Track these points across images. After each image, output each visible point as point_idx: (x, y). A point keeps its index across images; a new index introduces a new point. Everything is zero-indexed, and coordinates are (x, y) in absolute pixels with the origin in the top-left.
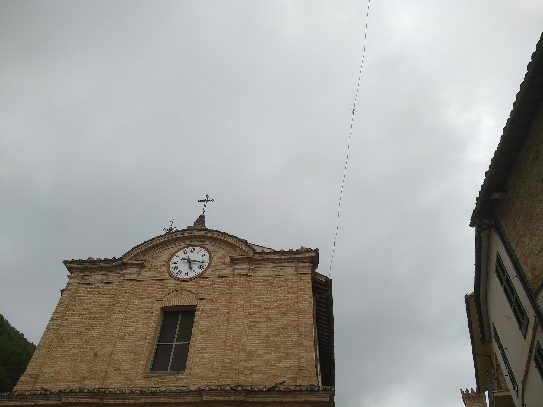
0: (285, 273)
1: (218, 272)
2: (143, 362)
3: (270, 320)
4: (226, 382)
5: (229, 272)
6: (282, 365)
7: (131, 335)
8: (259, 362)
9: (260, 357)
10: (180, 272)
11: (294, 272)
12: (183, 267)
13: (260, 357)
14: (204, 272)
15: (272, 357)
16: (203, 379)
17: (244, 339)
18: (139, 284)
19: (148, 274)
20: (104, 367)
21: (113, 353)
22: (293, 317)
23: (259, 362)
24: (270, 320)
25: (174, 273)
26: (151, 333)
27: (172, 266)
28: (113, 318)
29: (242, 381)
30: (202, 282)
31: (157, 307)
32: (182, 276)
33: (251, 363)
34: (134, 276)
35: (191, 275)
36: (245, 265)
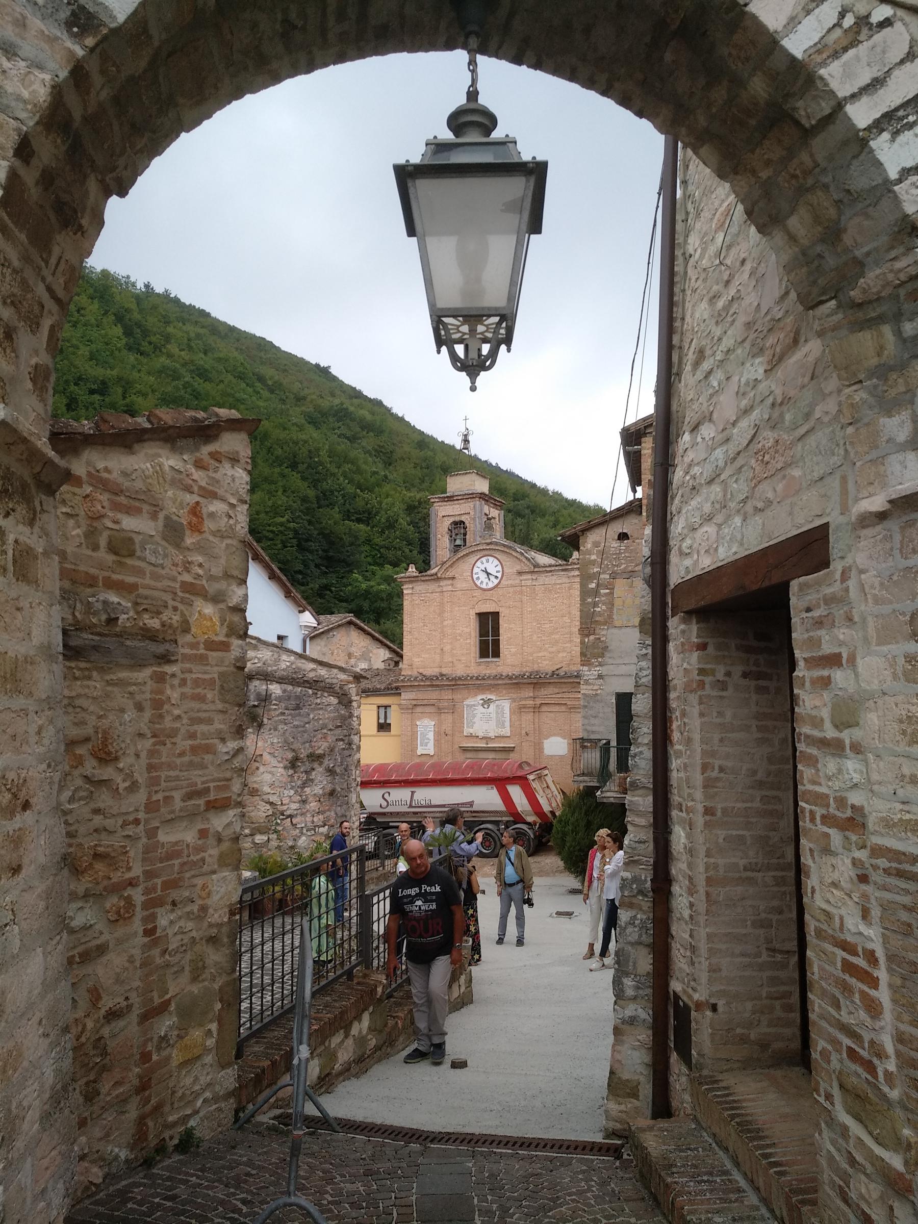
0: (560, 581)
1: (510, 582)
2: (473, 655)
3: (551, 622)
4: (527, 669)
5: (518, 581)
6: (560, 655)
7: (460, 635)
8: (545, 654)
9: (546, 650)
10: (482, 582)
11: (567, 580)
12: (483, 576)
13: (546, 650)
14: (500, 582)
15: (554, 649)
16: (512, 666)
17: (535, 638)
18: (455, 593)
19: (460, 584)
20: (450, 659)
21: (452, 649)
22: (566, 619)
23: (545, 654)
24: (551, 622)
25: (478, 583)
26: (473, 634)
27: (475, 577)
28: (446, 623)
29: (536, 667)
30: (500, 592)
31: (472, 614)
32: (484, 586)
33: (540, 654)
34: (450, 588)
35: (491, 585)
36: (529, 576)
